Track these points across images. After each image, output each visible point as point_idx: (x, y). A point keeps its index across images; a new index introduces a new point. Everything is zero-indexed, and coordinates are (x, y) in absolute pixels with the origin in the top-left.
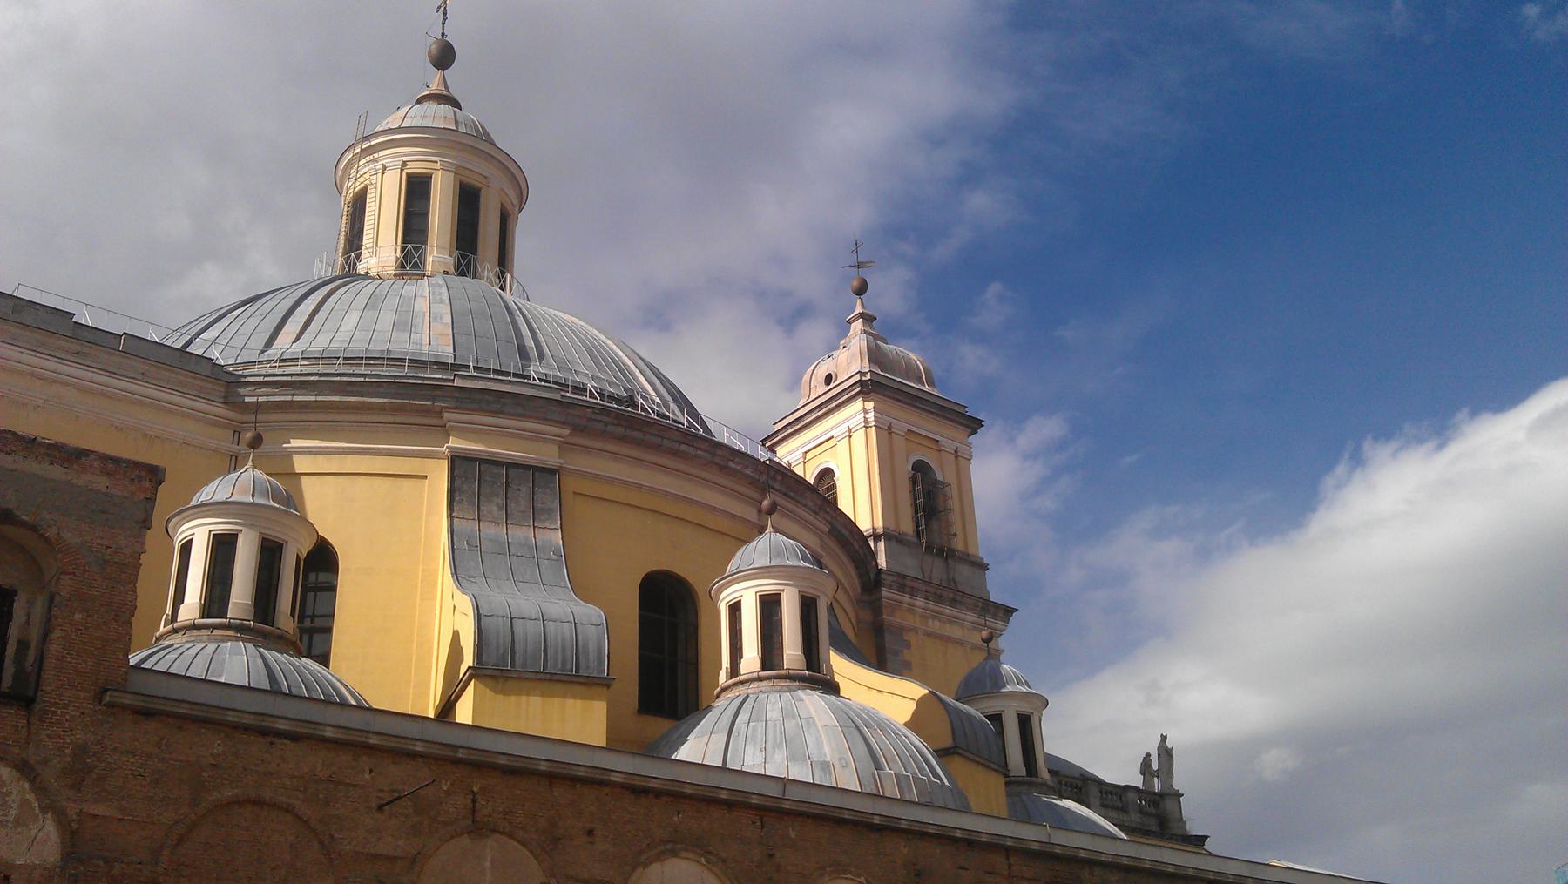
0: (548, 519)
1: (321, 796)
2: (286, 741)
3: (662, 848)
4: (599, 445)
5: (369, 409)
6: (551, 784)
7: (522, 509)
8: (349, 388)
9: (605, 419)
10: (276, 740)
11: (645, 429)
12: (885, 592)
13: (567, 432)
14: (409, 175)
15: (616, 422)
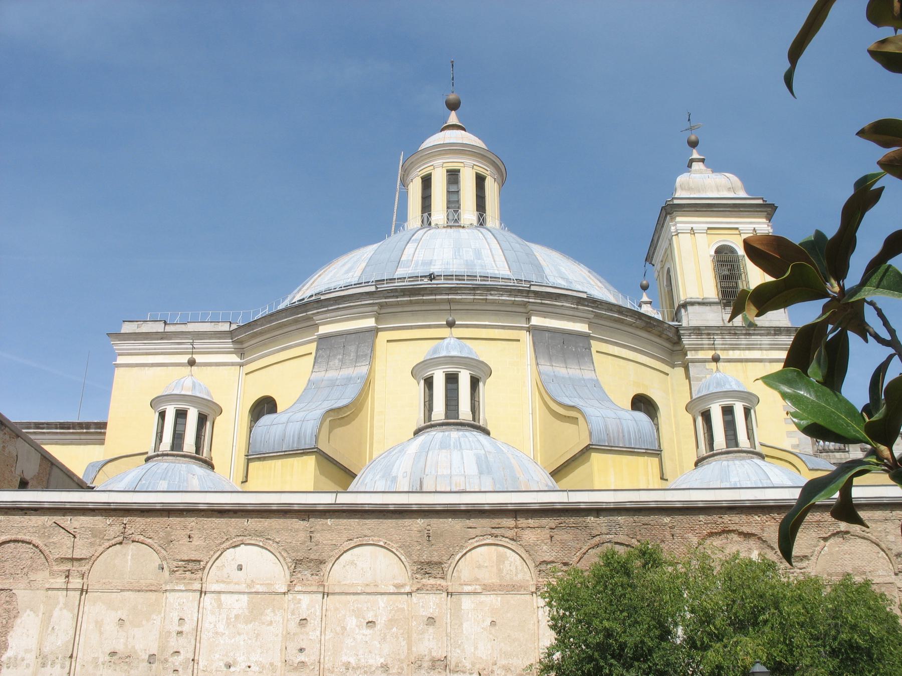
0: (365, 360)
1: (46, 534)
2: (32, 512)
3: (234, 540)
4: (400, 309)
5: (285, 325)
6: (169, 514)
7: (351, 358)
8: (272, 318)
9: (397, 294)
10: (26, 512)
11: (422, 293)
12: (686, 341)
13: (376, 308)
14: (422, 178)
15: (402, 294)
